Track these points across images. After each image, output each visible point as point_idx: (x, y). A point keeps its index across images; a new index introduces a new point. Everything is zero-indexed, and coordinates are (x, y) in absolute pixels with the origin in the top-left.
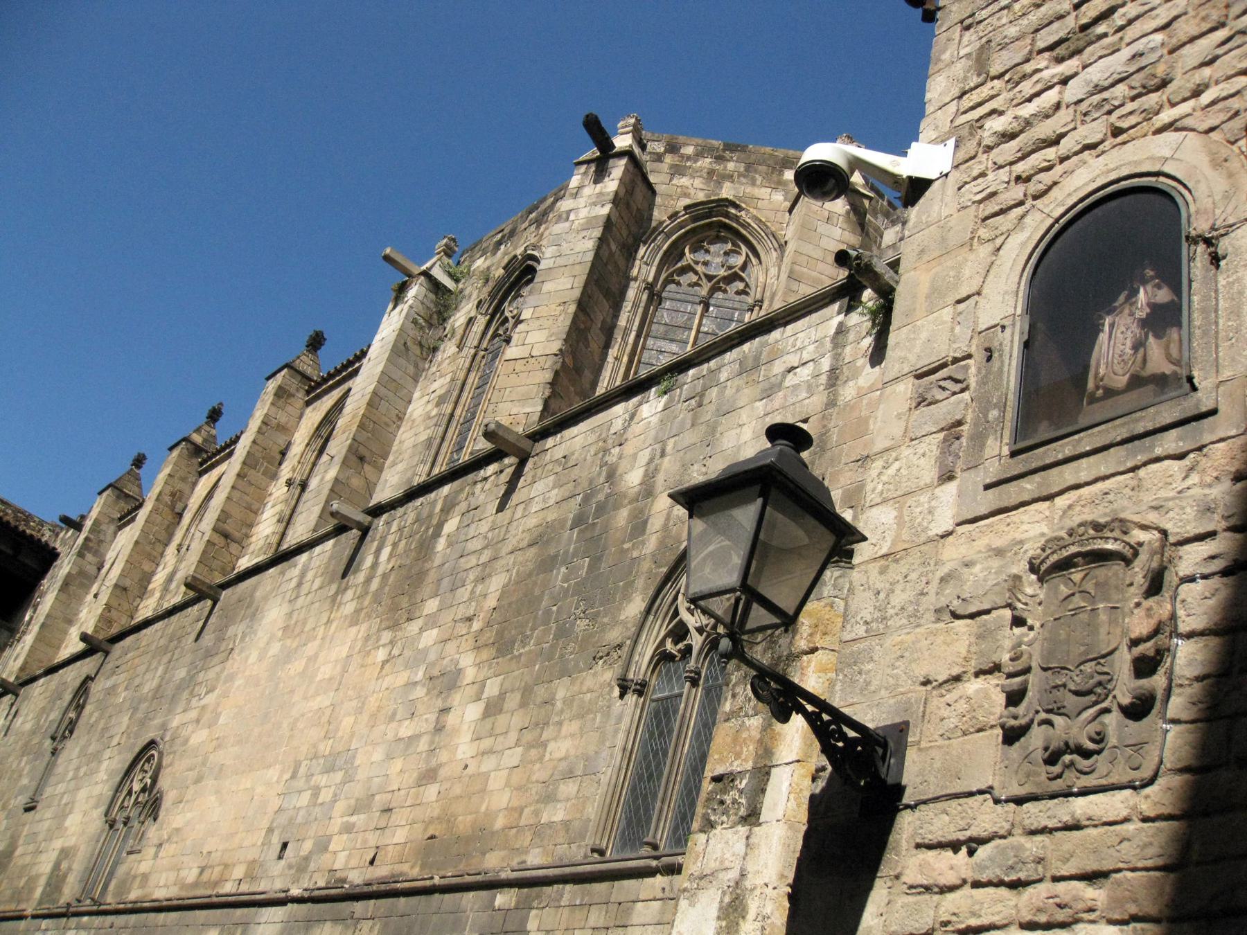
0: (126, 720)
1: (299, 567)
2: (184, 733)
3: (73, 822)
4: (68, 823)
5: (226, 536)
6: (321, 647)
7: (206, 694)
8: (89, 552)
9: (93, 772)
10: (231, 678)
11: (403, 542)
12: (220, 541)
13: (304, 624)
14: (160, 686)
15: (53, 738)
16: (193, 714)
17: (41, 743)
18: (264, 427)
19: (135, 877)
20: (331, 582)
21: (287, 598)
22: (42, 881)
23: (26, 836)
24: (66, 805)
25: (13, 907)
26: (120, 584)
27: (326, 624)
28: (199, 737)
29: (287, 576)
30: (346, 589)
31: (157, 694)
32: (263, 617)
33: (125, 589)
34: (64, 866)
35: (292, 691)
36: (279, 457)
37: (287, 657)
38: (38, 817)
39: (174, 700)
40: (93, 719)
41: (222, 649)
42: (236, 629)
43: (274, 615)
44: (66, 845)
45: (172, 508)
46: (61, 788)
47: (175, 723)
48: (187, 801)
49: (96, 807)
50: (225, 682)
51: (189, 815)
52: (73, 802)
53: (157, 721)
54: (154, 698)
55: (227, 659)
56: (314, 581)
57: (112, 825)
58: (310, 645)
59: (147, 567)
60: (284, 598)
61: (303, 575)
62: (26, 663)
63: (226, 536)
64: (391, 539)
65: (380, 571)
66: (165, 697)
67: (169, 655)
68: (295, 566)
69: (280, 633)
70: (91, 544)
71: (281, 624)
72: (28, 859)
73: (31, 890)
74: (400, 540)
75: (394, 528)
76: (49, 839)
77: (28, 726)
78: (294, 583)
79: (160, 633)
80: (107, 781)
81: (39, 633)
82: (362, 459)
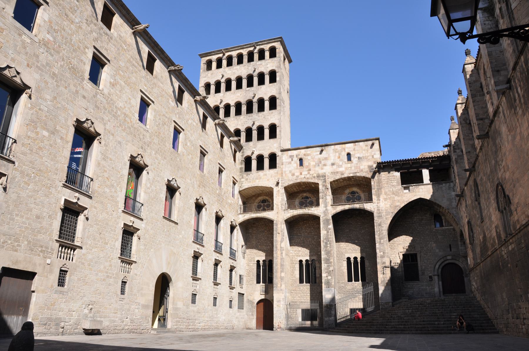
0: (489, 184)
1: (501, 112)
2: (503, 177)
3: (493, 218)
4: (492, 220)
5: (482, 119)
6: (520, 128)
7: (502, 163)
8: (456, 150)
9: (490, 203)
10: (505, 154)
11: (522, 83)
12: (481, 122)
13: (512, 125)
14: (491, 169)
15: (476, 200)
16: (502, 170)
17: (475, 204)
18: (471, 85)
19: (515, 222)
20: (511, 109)
21: (504, 122)
22: (496, 238)
23: (486, 229)
24: (489, 215)
25: (493, 249)
26: (467, 151)
27: (518, 121)
28: (507, 175)
29: (500, 117)
30: (516, 108)
31: (491, 171)
32: (502, 132)
33: (469, 152)
34: (498, 231)
35: (521, 146)
36: (481, 89)
37: (514, 138)
38: (485, 223)
39: (496, 170)
40: (482, 189)
41: (498, 148)
42: (498, 141)
43: (504, 129)
44: (495, 225)
45: (466, 123)
46: (486, 211)
47: (500, 176)
48: (515, 194)
49: (496, 211)
50: (504, 156)
51: (518, 197)
52: (491, 213)
53: (496, 179)
54: (491, 173)
55: (501, 150)
56: (507, 113)
57: (502, 212)
58: (517, 130)
59: (471, 142)
60: (503, 123)
61: (504, 114)
62: (460, 187)
63: (482, 119)
64: (518, 85)
65: (521, 96)
66: (494, 171)
67: (488, 160)
68: (500, 113)
69: (508, 133)
70: (456, 147)
71: (507, 130)
72: (489, 235)
73: (495, 242)
74: (520, 83)
75: (517, 82)
76: (491, 226)
77: (470, 202)
78: (503, 118)
79: (482, 156)
80: (494, 202)
81: (458, 178)
82: (498, 71)
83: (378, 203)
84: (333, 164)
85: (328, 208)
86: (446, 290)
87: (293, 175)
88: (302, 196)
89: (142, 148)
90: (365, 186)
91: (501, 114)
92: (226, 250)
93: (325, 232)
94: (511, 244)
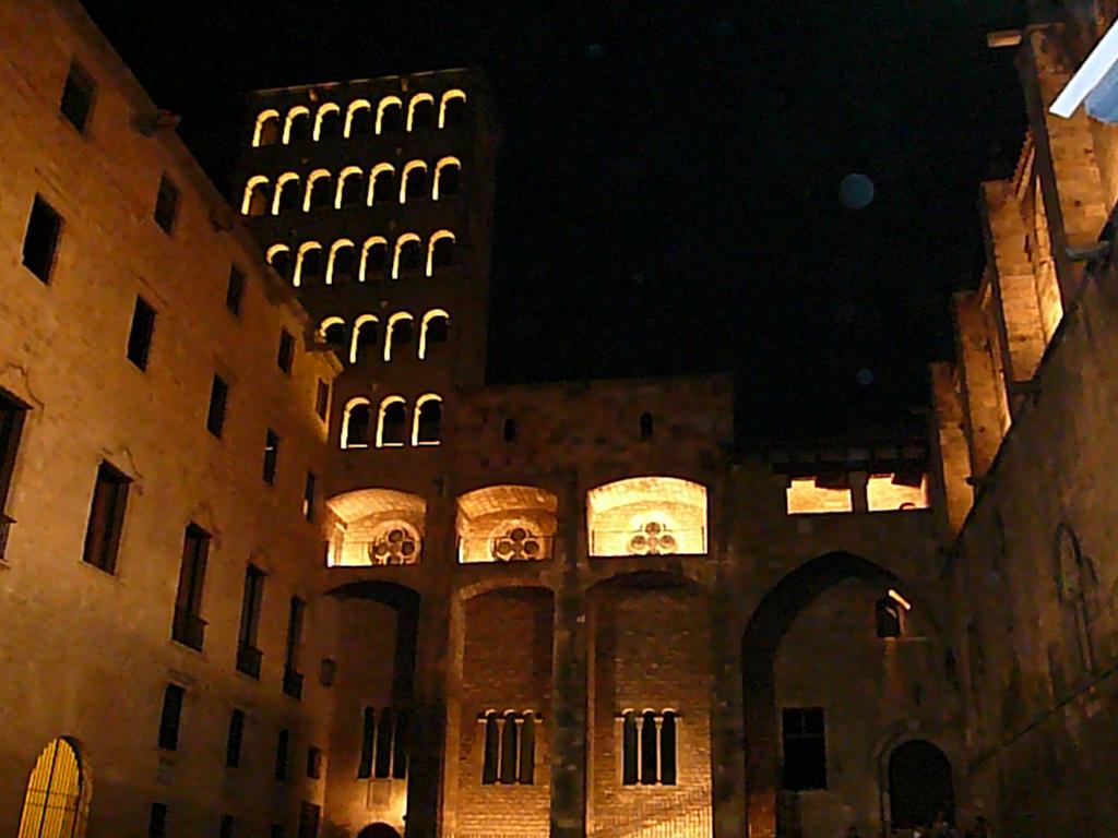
28: (1090, 499)
36: (1026, 256)
57: (1072, 605)
61: (1087, 321)
83: (719, 559)
84: (601, 441)
85: (578, 565)
86: (902, 817)
87: (485, 463)
88: (508, 525)
89: (27, 348)
90: (689, 510)
91: (1082, 325)
92: (273, 668)
93: (566, 634)
94: (1093, 697)
